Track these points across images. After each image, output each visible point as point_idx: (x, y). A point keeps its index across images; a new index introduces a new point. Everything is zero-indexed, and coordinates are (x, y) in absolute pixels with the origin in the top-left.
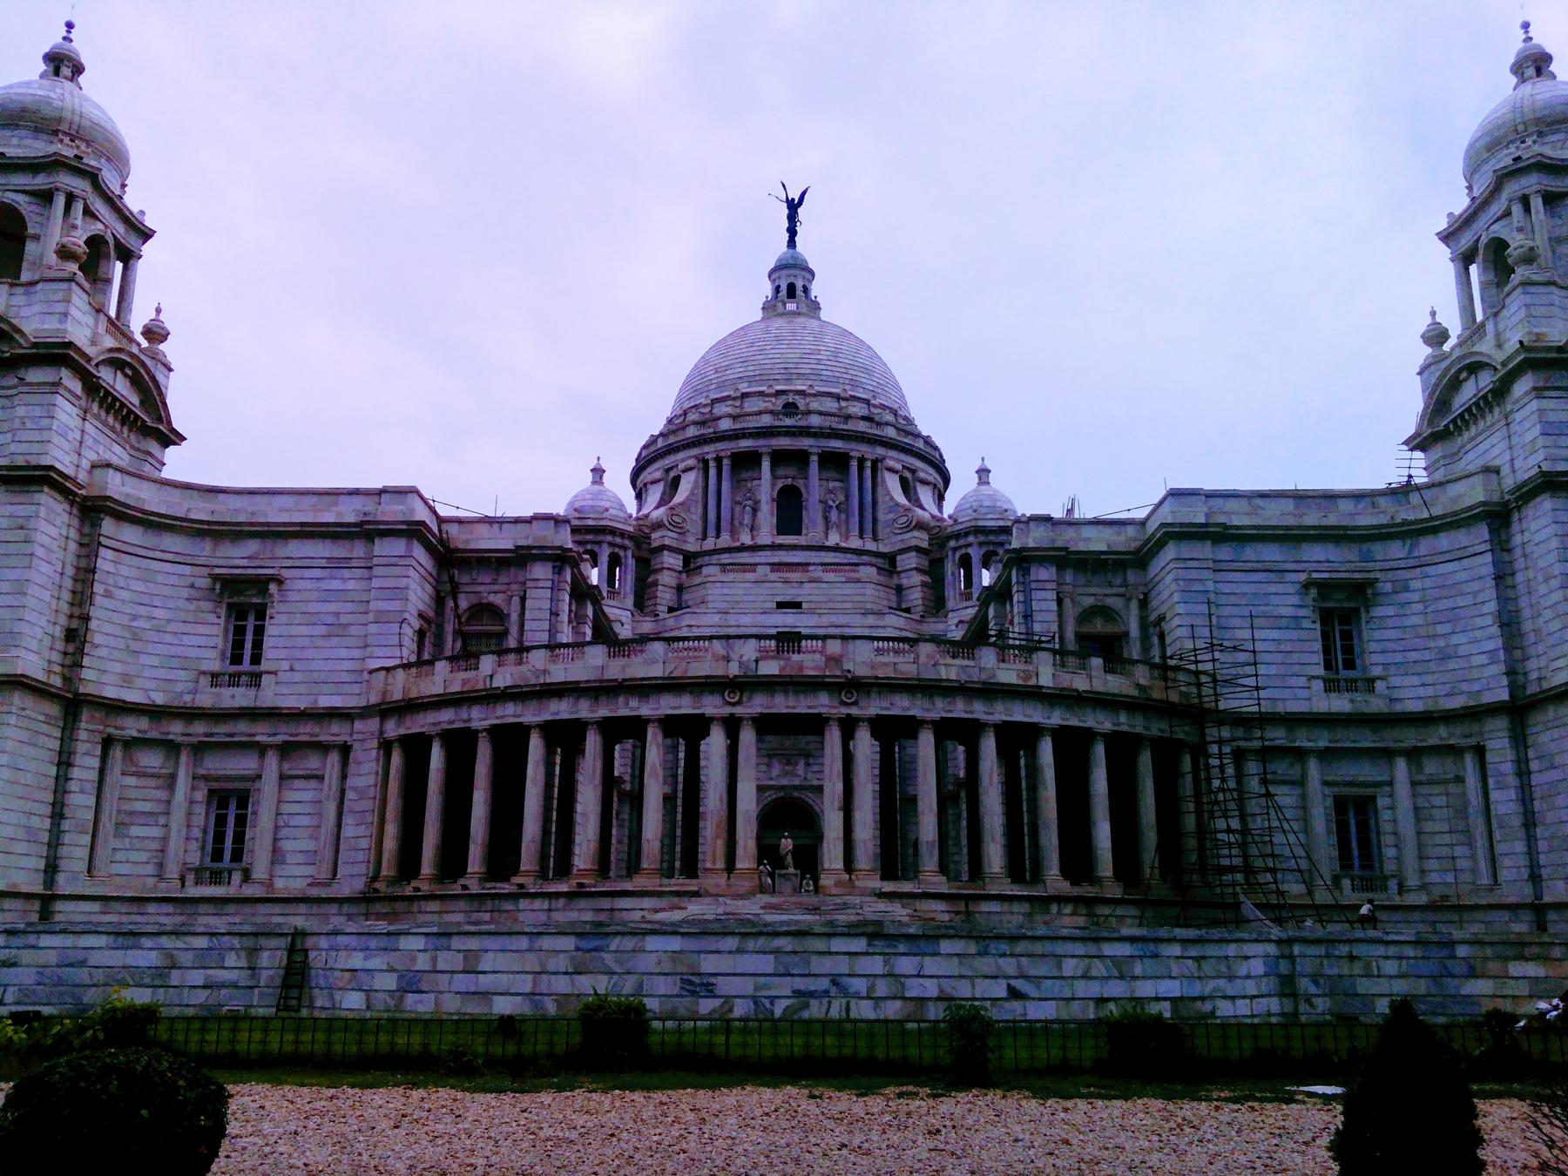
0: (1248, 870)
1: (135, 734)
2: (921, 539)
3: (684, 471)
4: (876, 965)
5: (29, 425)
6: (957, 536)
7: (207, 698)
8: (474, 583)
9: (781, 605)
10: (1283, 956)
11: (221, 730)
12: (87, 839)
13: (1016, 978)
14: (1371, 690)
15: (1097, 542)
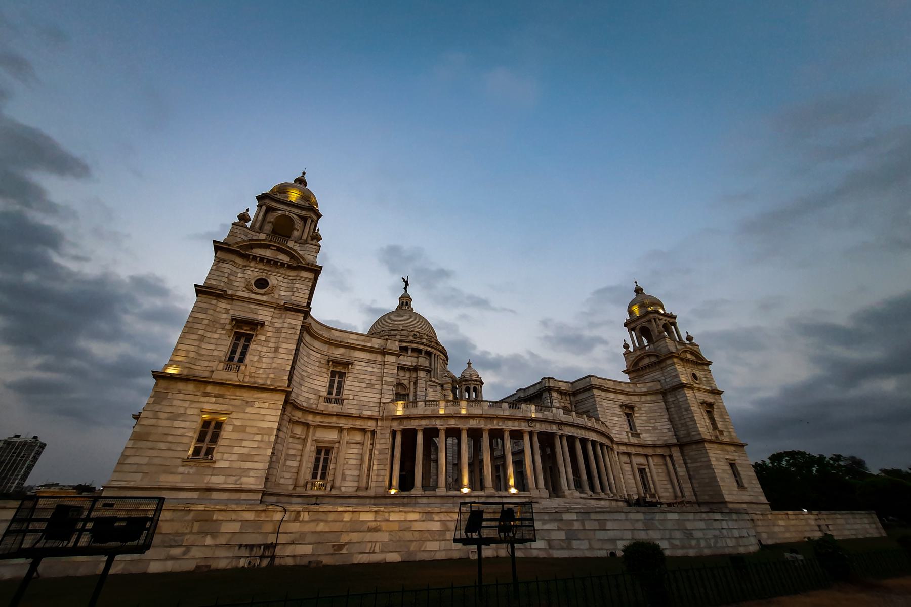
1: (296, 419)
7: (322, 406)
11: (326, 420)
14: (640, 437)
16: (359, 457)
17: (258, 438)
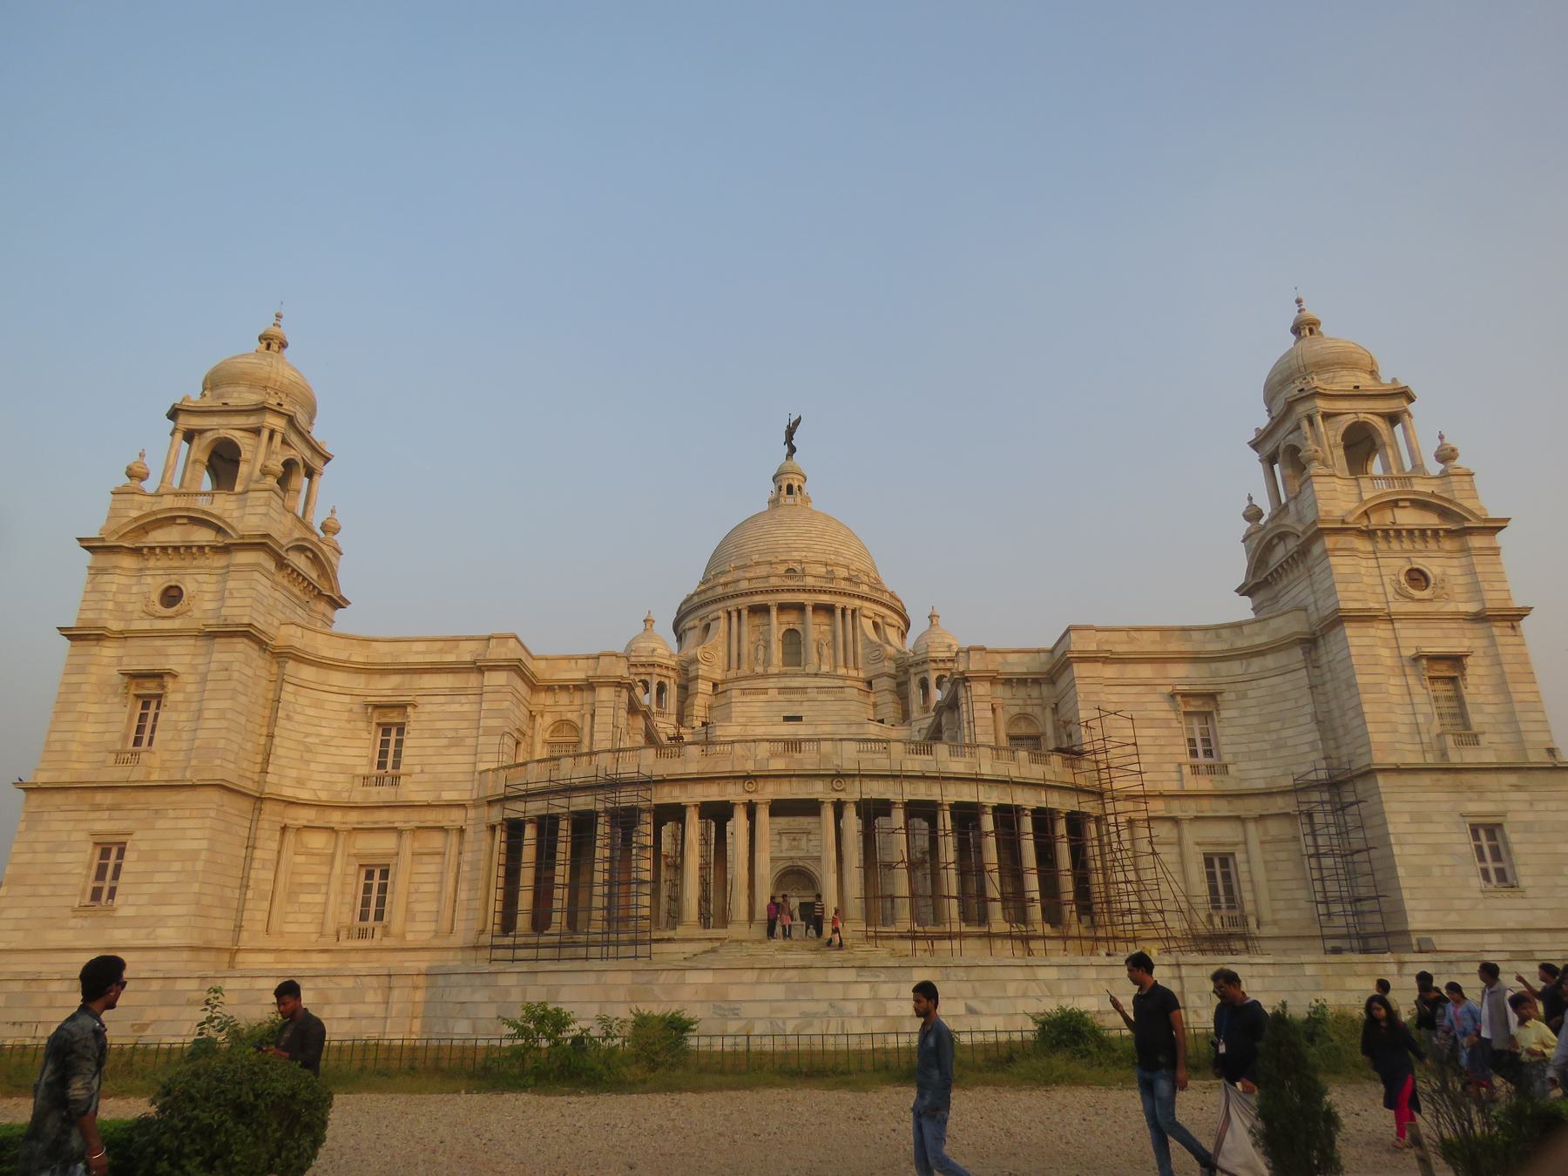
0: (1144, 913)
1: (305, 823)
2: (889, 667)
3: (713, 620)
4: (863, 991)
5: (235, 594)
6: (917, 664)
7: (358, 797)
8: (556, 704)
9: (787, 719)
10: (1174, 978)
11: (368, 819)
12: (266, 905)
13: (970, 998)
15: (1017, 665)
16: (437, 879)
17: (177, 866)
